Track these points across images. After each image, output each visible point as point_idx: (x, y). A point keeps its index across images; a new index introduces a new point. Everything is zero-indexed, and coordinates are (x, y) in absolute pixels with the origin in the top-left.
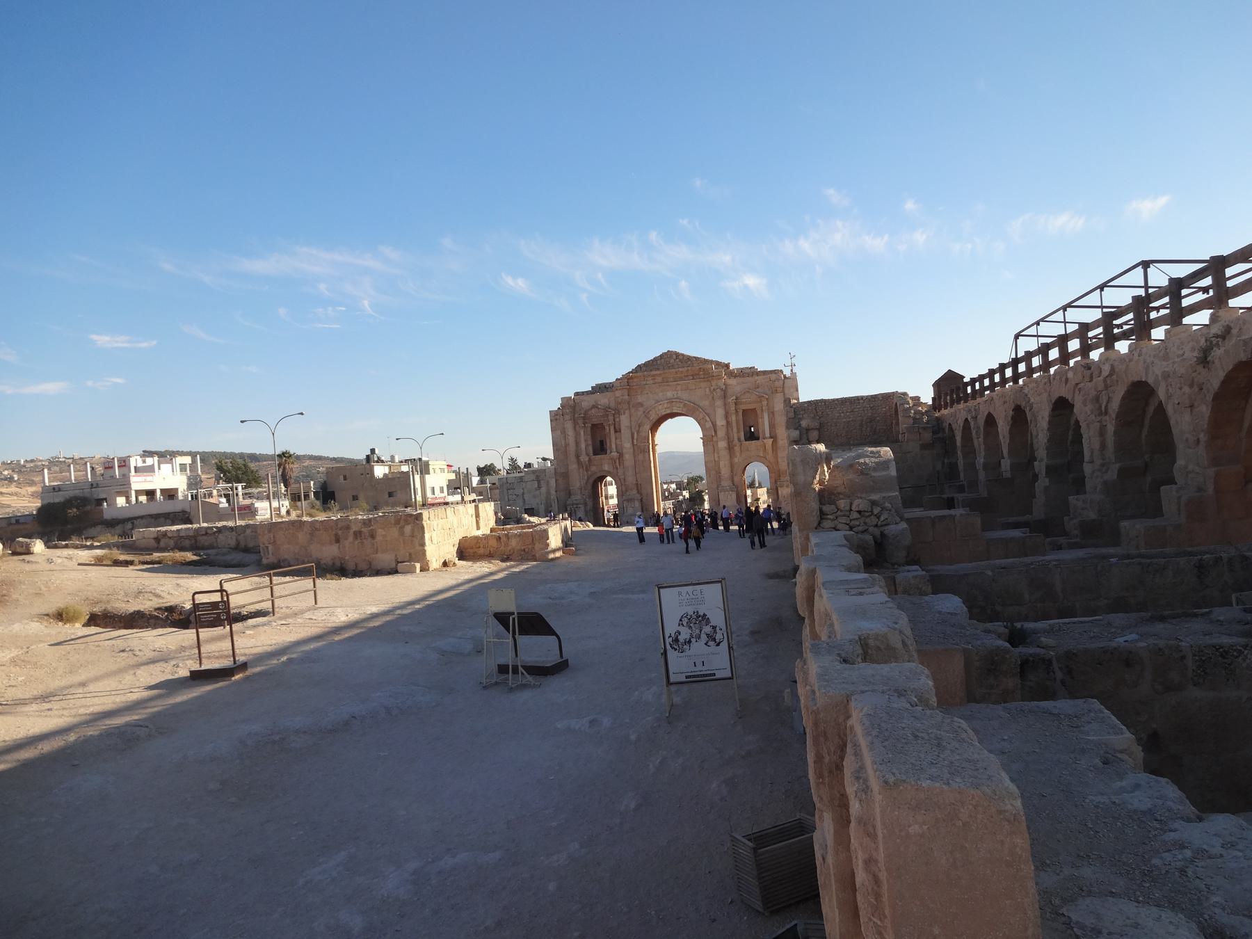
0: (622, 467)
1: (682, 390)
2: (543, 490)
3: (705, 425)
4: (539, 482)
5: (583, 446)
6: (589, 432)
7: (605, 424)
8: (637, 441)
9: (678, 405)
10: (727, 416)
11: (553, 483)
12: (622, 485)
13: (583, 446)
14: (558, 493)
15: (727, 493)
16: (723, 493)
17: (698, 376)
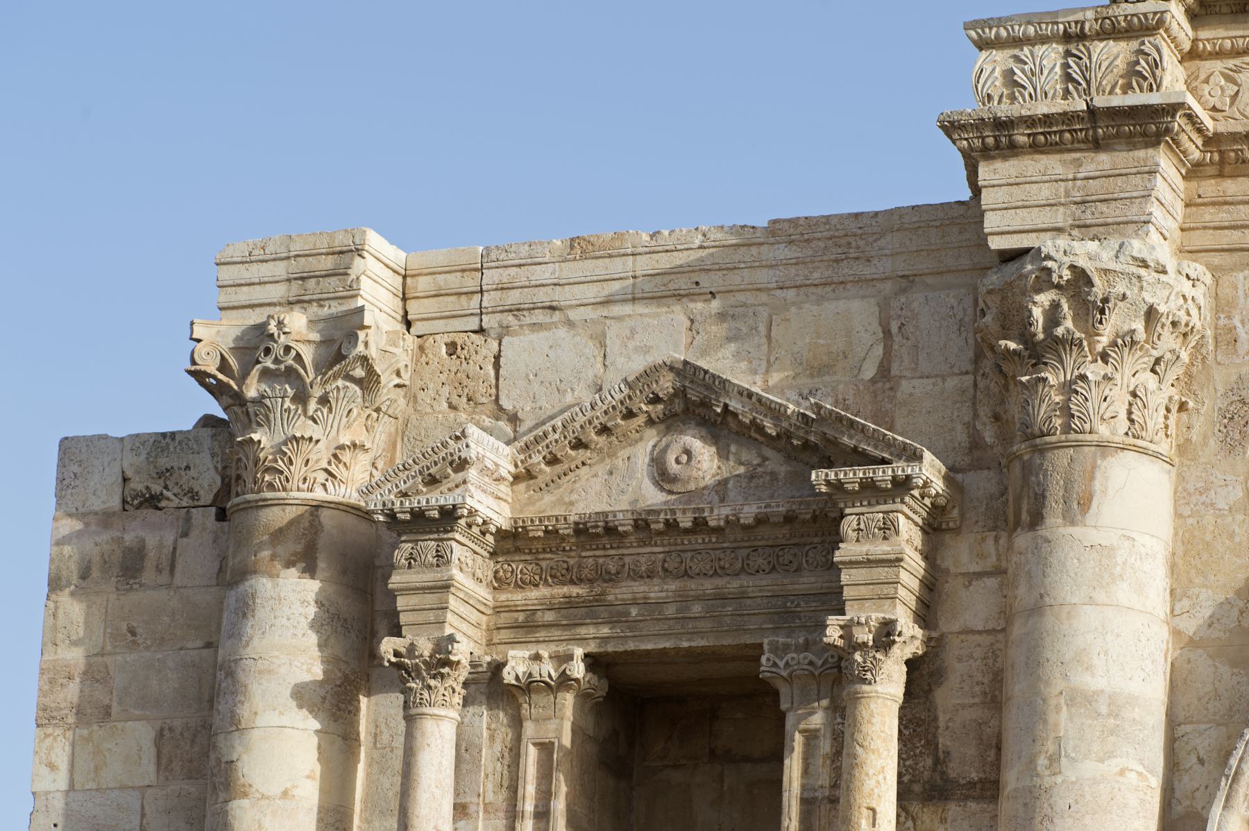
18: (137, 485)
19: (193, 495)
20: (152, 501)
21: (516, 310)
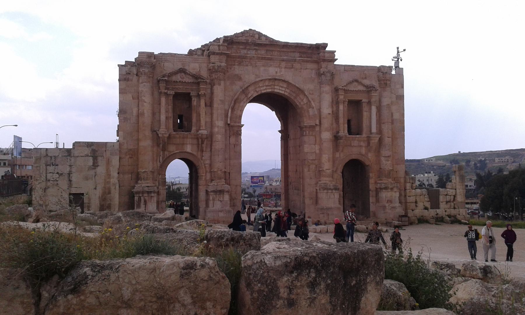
0: (209, 150)
1: (285, 68)
2: (101, 170)
3: (308, 111)
4: (95, 158)
5: (163, 117)
6: (171, 102)
7: (193, 94)
8: (230, 120)
9: (281, 84)
10: (335, 103)
11: (115, 161)
12: (206, 172)
13: (163, 117)
14: (121, 175)
15: (330, 191)
16: (326, 191)
17: (305, 55)
18: (128, 72)
19: (134, 74)
20: (129, 74)
21: (165, 61)
